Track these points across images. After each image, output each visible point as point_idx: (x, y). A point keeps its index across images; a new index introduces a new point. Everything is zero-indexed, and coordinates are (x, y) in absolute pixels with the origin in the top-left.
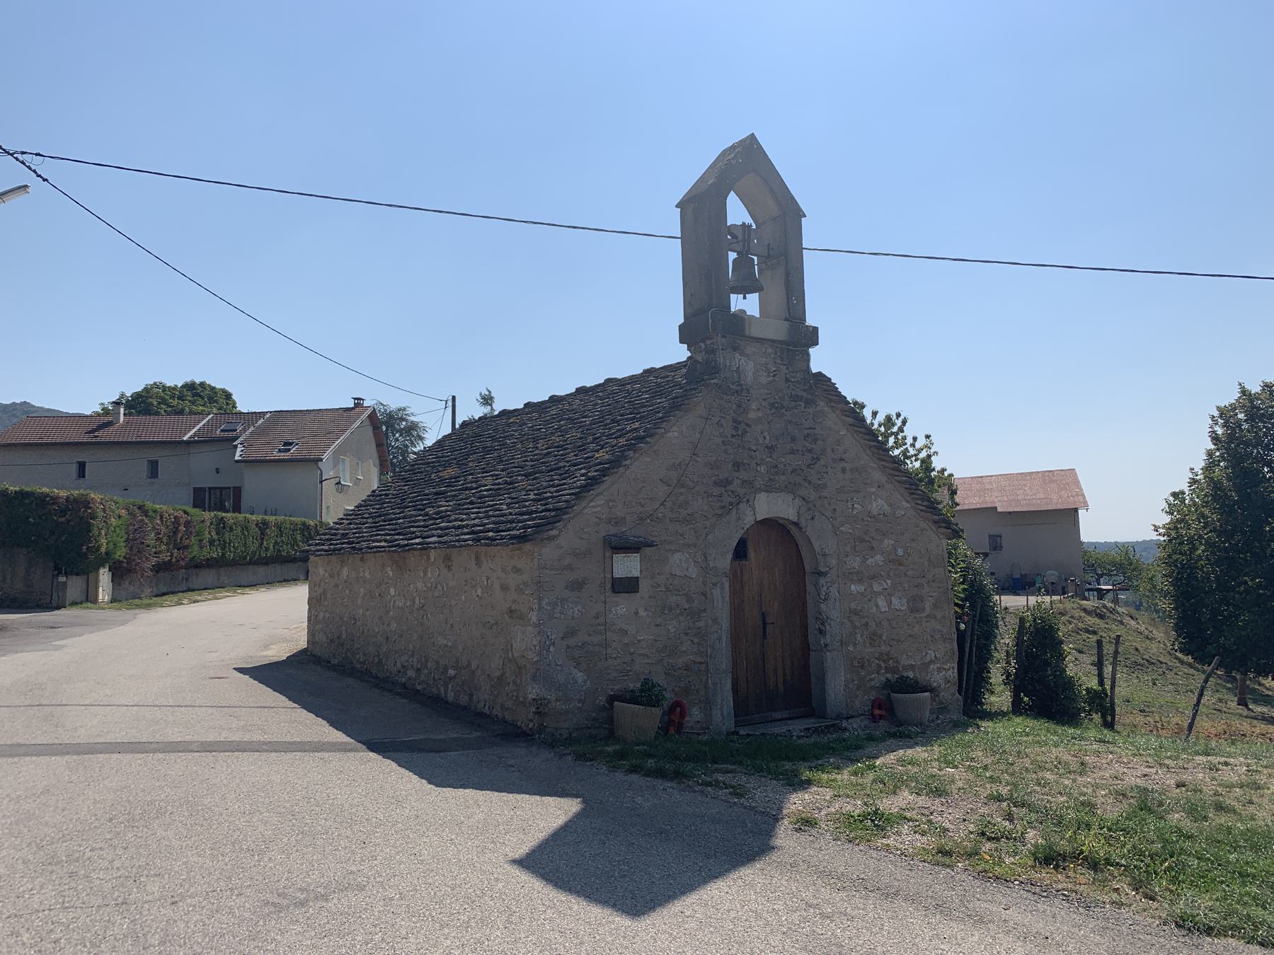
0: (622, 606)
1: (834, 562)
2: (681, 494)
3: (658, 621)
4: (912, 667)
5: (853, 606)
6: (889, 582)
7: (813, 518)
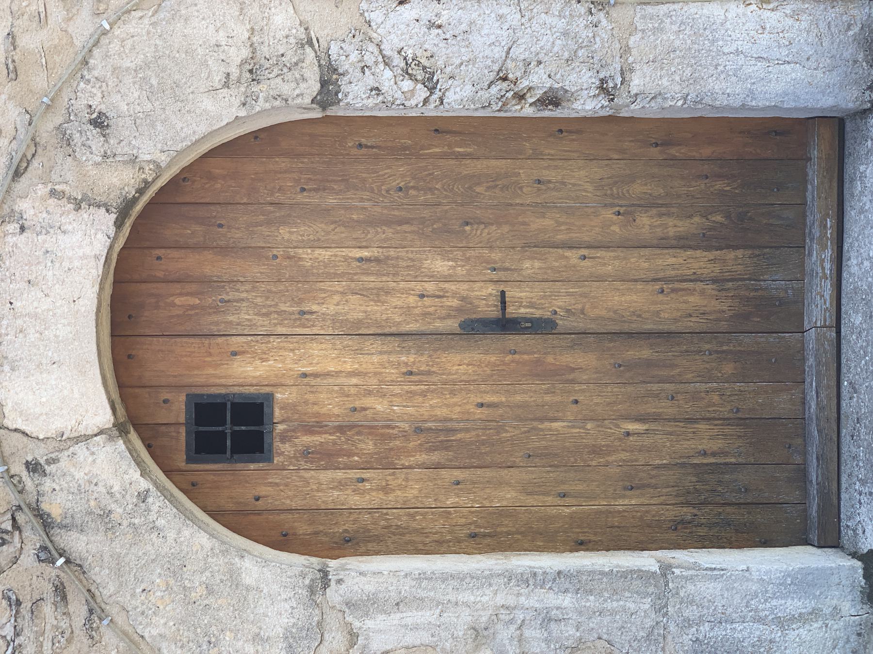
7: (100, 122)
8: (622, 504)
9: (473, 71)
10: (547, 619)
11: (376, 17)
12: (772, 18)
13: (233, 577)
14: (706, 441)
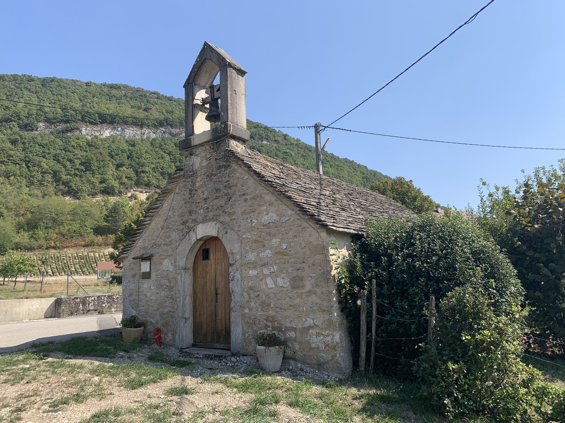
0: (146, 284)
2: (167, 232)
4: (294, 329)
5: (250, 284)
6: (275, 267)
7: (226, 233)
12: (240, 336)
13: (184, 257)
14: (205, 327)
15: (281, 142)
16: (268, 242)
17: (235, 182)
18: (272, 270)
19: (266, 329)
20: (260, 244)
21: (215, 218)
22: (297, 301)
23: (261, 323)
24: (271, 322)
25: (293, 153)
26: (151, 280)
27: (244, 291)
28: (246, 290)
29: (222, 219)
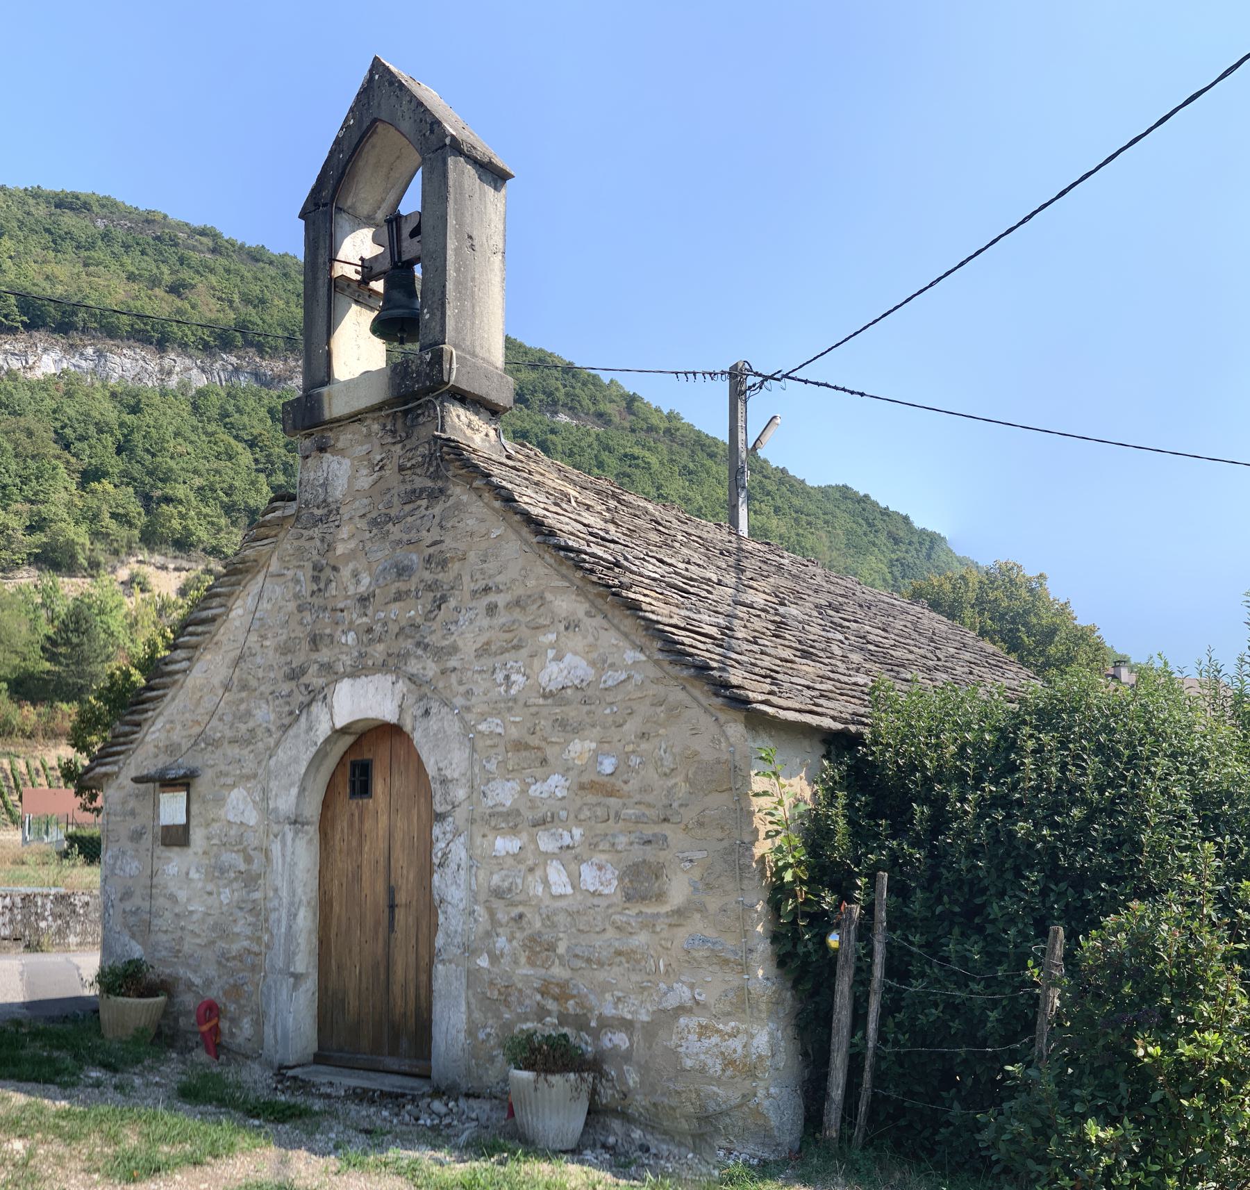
0: (175, 864)
1: (461, 793)
2: (242, 701)
3: (210, 887)
5: (496, 879)
6: (577, 832)
8: (333, 962)
9: (443, 886)
10: (279, 921)
11: (462, 839)
12: (462, 1036)
13: (292, 785)
14: (353, 1002)
15: (616, 420)
16: (557, 748)
17: (462, 546)
18: (567, 840)
19: (541, 1020)
20: (529, 754)
21: (391, 662)
22: (641, 939)
23: (527, 1002)
24: (556, 999)
25: (653, 460)
26: (190, 851)
27: (476, 902)
28: (482, 897)
29: (413, 667)
